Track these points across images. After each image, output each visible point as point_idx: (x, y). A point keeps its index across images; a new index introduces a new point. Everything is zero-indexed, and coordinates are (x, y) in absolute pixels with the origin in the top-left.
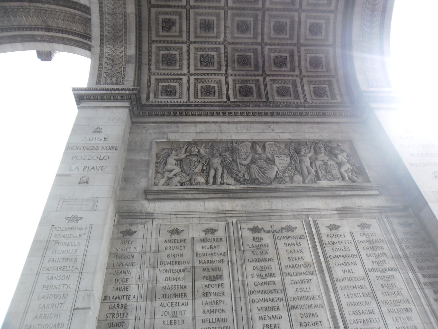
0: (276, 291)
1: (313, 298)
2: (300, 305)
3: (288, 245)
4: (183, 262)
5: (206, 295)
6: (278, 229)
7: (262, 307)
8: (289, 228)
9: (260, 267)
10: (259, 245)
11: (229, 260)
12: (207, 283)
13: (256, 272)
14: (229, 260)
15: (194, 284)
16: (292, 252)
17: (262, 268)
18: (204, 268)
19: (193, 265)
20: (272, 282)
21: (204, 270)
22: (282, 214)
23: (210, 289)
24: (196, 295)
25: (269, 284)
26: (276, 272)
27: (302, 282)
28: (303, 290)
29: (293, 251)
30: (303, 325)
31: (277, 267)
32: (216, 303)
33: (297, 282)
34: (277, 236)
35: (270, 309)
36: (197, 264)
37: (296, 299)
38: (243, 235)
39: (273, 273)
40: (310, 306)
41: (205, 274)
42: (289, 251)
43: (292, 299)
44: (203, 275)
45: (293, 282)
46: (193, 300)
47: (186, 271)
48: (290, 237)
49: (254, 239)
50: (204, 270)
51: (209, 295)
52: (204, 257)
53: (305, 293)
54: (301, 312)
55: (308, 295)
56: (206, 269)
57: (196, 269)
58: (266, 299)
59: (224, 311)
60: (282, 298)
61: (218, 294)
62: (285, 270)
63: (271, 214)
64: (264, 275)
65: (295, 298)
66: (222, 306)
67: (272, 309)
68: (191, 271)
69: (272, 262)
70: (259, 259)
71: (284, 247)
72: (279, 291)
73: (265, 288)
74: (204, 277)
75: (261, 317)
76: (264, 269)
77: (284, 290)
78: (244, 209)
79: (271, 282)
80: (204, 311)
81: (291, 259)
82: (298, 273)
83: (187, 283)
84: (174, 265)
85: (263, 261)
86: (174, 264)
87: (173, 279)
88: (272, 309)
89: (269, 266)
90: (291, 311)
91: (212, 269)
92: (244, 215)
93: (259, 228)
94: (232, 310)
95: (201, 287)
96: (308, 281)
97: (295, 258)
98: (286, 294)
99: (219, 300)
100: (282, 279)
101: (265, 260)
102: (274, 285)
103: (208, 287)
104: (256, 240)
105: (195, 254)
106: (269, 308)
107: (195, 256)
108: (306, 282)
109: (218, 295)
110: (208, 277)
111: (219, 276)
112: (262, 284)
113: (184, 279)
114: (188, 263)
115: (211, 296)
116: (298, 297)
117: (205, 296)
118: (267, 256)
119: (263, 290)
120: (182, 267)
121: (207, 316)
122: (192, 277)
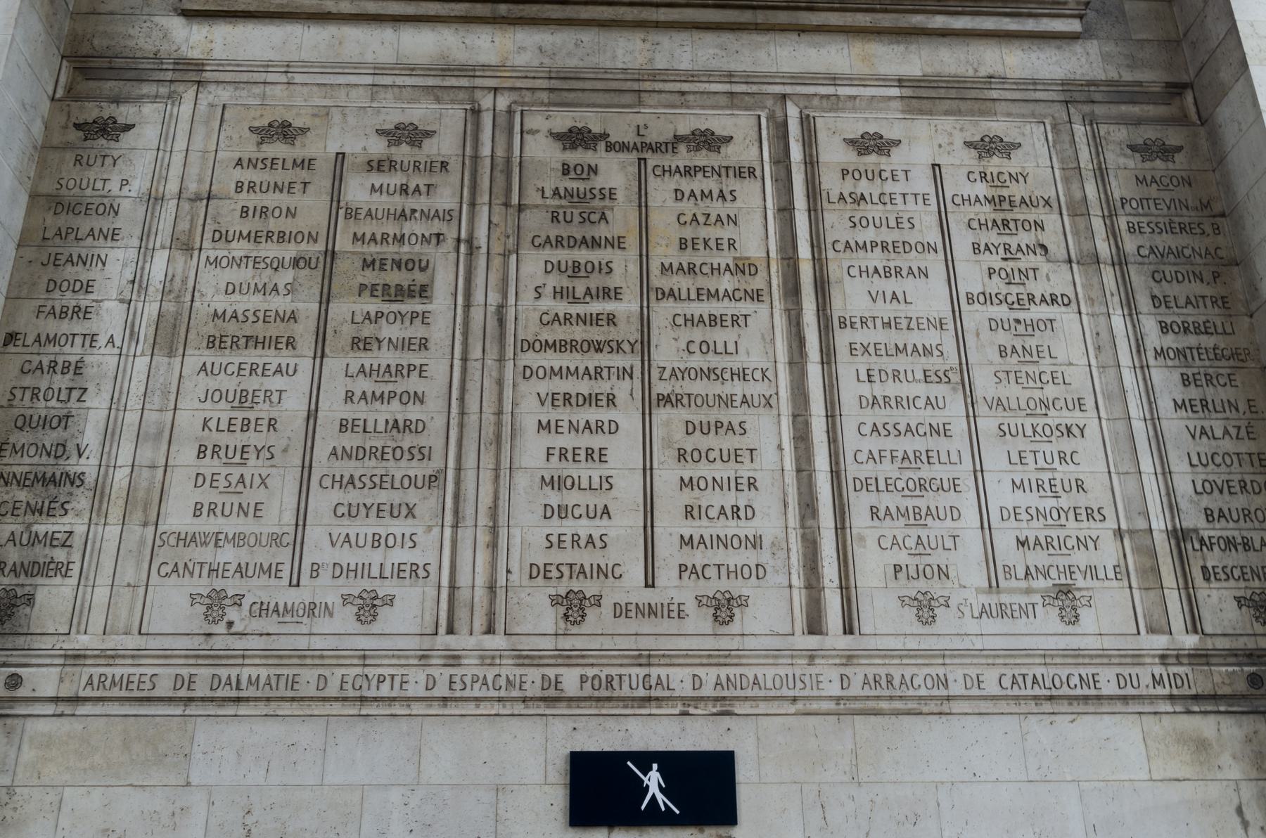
0: (614, 344)
1: (742, 375)
2: (689, 395)
3: (687, 195)
4: (293, 235)
5: (362, 347)
6: (661, 140)
7: (553, 394)
8: (703, 139)
9: (570, 264)
10: (582, 190)
11: (463, 235)
12: (373, 306)
13: (553, 281)
14: (463, 235)
15: (327, 311)
16: (697, 220)
17: (576, 270)
18: (369, 259)
19: (330, 247)
20: (604, 317)
21: (367, 264)
22: (685, 87)
23: (380, 328)
24: (327, 343)
25: (594, 322)
26: (623, 285)
27: (713, 323)
28: (712, 347)
29: (701, 219)
30: (689, 458)
31: (634, 269)
32: (393, 373)
33: (696, 321)
34: (651, 164)
35: (581, 402)
36: (343, 243)
37: (679, 375)
38: (528, 153)
39: (616, 288)
40: (728, 401)
41: (370, 277)
42: (688, 218)
43: (666, 375)
44: (361, 280)
45: (680, 321)
46: (314, 358)
47: (302, 264)
48: (703, 169)
49: (566, 170)
50: (367, 264)
51: (375, 346)
52: (374, 221)
53: (718, 358)
54: (690, 418)
55: (729, 365)
56: (373, 262)
57: (337, 261)
58: (572, 369)
59: (419, 398)
60: (632, 368)
61: (406, 345)
62: (657, 281)
63: (647, 86)
64: (580, 291)
65: (677, 370)
66: (413, 383)
67: (587, 402)
68: (321, 265)
69: (619, 252)
70: (572, 240)
71: (670, 202)
72: (626, 347)
73: (578, 333)
74: (362, 287)
75: (544, 423)
76: (583, 273)
77: (644, 345)
78: (547, 61)
79: (600, 317)
80: (350, 394)
81: (689, 243)
82: (705, 292)
83: (300, 306)
84: (263, 245)
85: (583, 246)
86: (263, 240)
87: (252, 290)
88: (587, 402)
89: (604, 262)
90: (653, 412)
91: (398, 264)
93: (590, 131)
94: (447, 395)
95: (349, 319)
96: (735, 320)
97: (706, 242)
98: (646, 358)
99: (405, 364)
100: (642, 307)
101: (595, 243)
102: (612, 328)
103: (373, 318)
105: (342, 212)
106: (581, 398)
107: (341, 219)
108: (729, 323)
109: (406, 348)
110: (380, 288)
111: (417, 288)
112: (567, 318)
113: (291, 289)
114: (311, 240)
115: (379, 349)
116: (688, 370)
117: (359, 349)
118: (602, 231)
119: (569, 341)
120: (289, 251)
121: (360, 411)
122: (320, 286)
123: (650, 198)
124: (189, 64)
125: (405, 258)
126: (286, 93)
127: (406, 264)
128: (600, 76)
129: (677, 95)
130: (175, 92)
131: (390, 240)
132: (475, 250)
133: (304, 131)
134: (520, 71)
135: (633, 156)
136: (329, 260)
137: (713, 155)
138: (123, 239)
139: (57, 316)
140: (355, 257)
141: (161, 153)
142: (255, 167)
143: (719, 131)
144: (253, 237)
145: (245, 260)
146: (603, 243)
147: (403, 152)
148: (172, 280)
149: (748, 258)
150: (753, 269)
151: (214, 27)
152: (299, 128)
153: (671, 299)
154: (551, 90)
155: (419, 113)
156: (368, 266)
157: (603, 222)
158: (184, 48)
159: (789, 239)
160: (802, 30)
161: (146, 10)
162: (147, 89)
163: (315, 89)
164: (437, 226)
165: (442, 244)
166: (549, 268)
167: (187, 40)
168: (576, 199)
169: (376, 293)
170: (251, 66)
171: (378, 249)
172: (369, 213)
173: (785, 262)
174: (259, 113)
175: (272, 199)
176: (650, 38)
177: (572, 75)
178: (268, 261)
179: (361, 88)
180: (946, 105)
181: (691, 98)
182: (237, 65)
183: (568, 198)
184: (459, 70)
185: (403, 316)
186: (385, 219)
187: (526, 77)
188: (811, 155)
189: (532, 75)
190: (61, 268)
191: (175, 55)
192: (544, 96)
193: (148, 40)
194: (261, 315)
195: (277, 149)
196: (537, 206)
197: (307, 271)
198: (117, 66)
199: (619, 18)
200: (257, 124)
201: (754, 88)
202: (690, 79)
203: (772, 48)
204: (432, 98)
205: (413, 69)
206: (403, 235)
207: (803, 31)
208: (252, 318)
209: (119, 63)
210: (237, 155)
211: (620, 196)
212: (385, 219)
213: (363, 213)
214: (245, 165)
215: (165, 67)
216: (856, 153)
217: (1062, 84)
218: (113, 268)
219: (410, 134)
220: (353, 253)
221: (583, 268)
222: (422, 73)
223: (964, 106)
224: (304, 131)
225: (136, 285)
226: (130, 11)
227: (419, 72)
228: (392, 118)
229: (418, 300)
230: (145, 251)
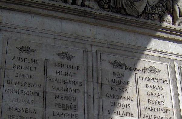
10: (119, 81)
12: (60, 111)
14: (86, 91)
18: (57, 95)
21: (57, 97)
29: (154, 94)
31: (136, 108)
34: (139, 75)
36: (49, 89)
42: (150, 94)
47: (36, 94)
48: (153, 79)
50: (57, 97)
56: (59, 96)
68: (42, 95)
69: (131, 102)
81: (151, 101)
82: (156, 117)
86: (23, 85)
87: (21, 101)
89: (127, 105)
91: (66, 98)
92: (106, 45)
104: (116, 76)
110: (61, 105)
113: (34, 102)
125: (68, 96)
131: (63, 90)
136: (45, 94)
137: (156, 75)
143: (157, 68)
144: (21, 84)
145: (18, 91)
146: (127, 98)
149: (168, 108)
150: (169, 111)
153: (147, 118)
156: (57, 98)
159: (178, 103)
166: (112, 104)
168: (118, 83)
169: (60, 106)
171: (60, 92)
172: (56, 80)
173: (177, 110)
183: (116, 83)
185: (69, 115)
194: (24, 110)
196: (107, 84)
197: (38, 97)
208: (22, 111)
214: (16, 59)
220: (53, 93)
221: (121, 106)
229: (73, 110)
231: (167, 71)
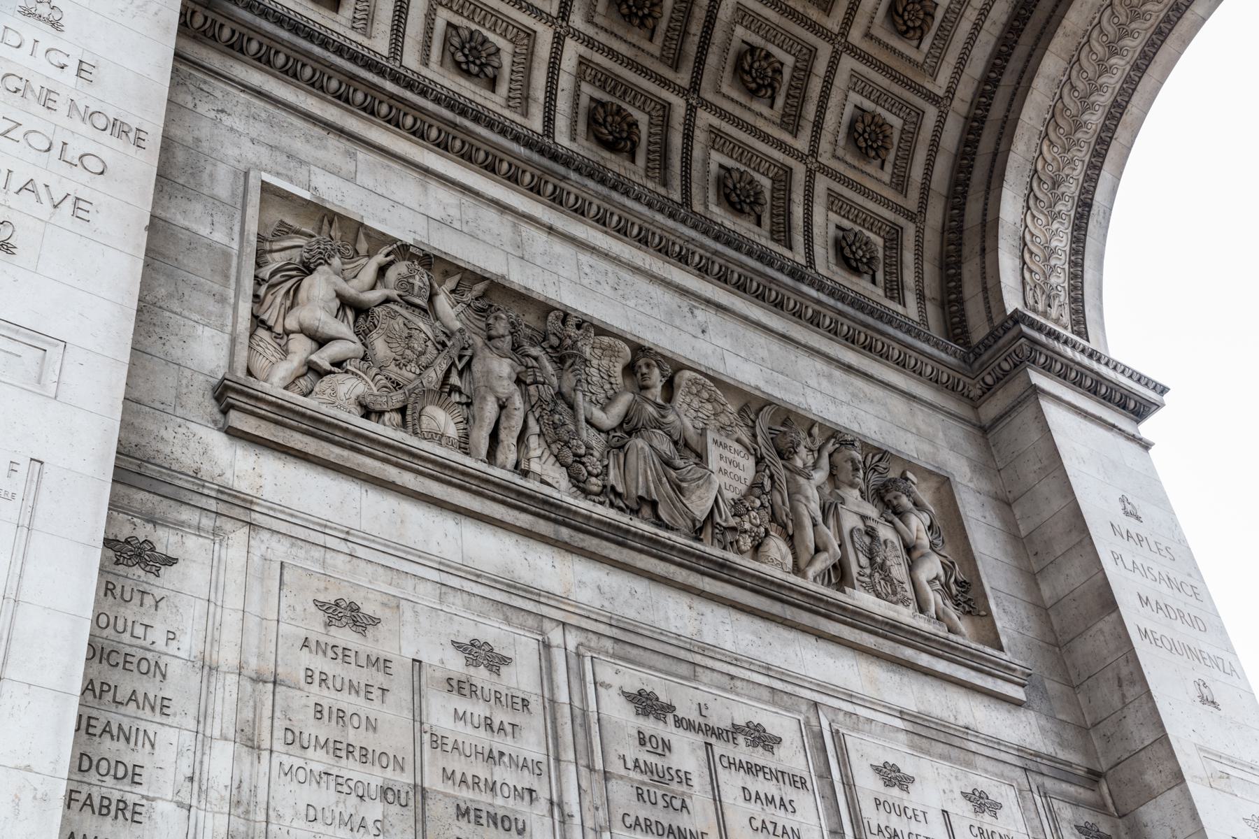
14: (555, 799)
19: (418, 781)
21: (462, 813)
52: (463, 757)
56: (467, 811)
84: (344, 762)
105: (426, 737)
107: (427, 747)
120: (375, 777)
123: (722, 793)
124: (235, 497)
126: (348, 567)
127: (503, 821)
128: (656, 636)
129: (727, 677)
130: (220, 528)
132: (567, 818)
133: (375, 621)
134: (584, 609)
135: (700, 739)
138: (175, 715)
139: (97, 811)
140: (447, 800)
141: (212, 606)
142: (325, 653)
147: (481, 676)
148: (239, 787)
151: (262, 459)
152: (370, 617)
154: (616, 640)
155: (493, 631)
157: (684, 810)
158: (229, 474)
160: (820, 635)
161: (179, 411)
162: (186, 515)
163: (381, 570)
164: (526, 780)
165: (535, 803)
167: (232, 466)
168: (656, 778)
170: (307, 520)
174: (322, 585)
175: (349, 702)
176: (694, 605)
177: (631, 628)
178: (352, 784)
179: (429, 583)
180: (940, 748)
181: (739, 683)
182: (291, 517)
183: (649, 774)
184: (525, 591)
186: (473, 757)
187: (588, 618)
188: (847, 776)
189: (594, 616)
190: (97, 739)
191: (218, 480)
192: (609, 644)
193: (185, 450)
195: (345, 636)
196: (621, 777)
198: (148, 473)
199: (671, 576)
200: (321, 598)
201: (789, 688)
202: (734, 662)
203: (798, 649)
204: (501, 616)
205: (478, 576)
206: (495, 783)
207: (820, 637)
209: (151, 470)
210: (303, 634)
211: (695, 781)
212: (473, 757)
213: (450, 742)
215: (206, 491)
216: (881, 783)
217: (1018, 750)
218: (165, 754)
219: (477, 652)
222: (487, 583)
223: (955, 753)
224: (375, 621)
225: (196, 785)
226: (162, 407)
227: (484, 581)
228: (467, 633)
230: (203, 739)
231: (800, 744)
